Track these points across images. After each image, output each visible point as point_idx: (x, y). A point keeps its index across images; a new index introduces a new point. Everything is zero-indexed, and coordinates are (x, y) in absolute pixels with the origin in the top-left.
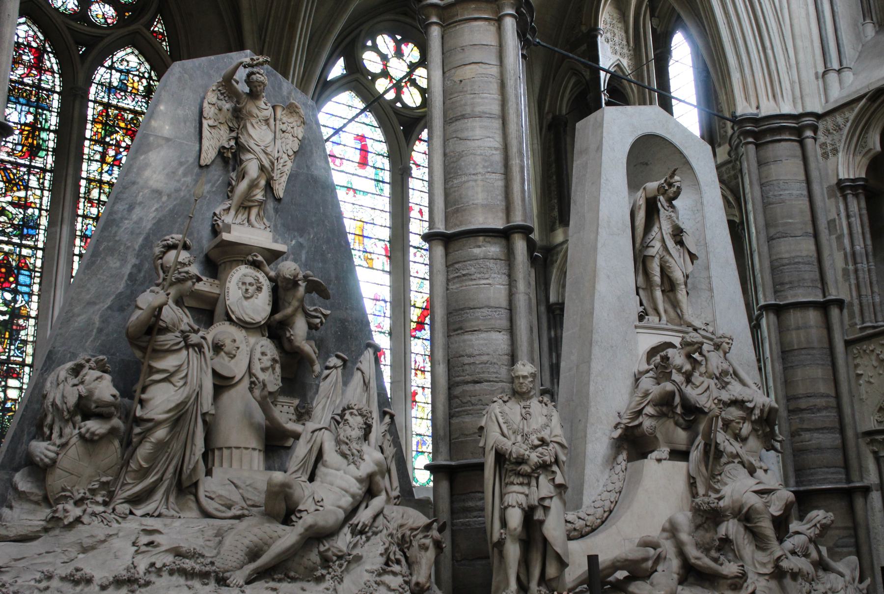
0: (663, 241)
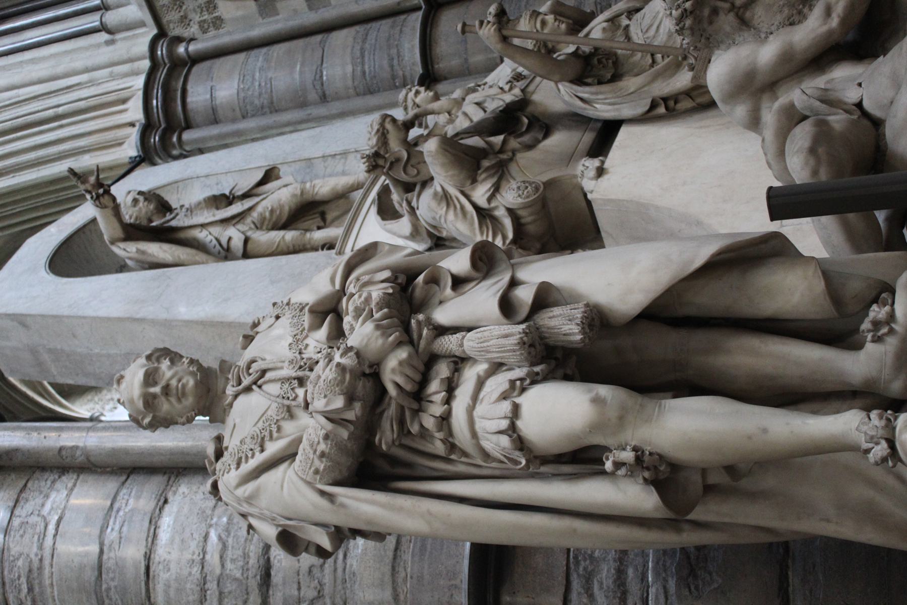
0: (225, 221)
